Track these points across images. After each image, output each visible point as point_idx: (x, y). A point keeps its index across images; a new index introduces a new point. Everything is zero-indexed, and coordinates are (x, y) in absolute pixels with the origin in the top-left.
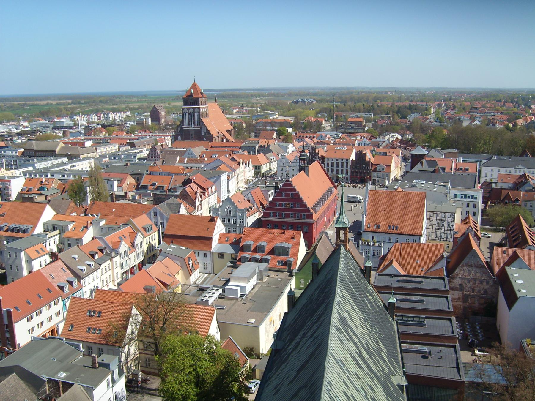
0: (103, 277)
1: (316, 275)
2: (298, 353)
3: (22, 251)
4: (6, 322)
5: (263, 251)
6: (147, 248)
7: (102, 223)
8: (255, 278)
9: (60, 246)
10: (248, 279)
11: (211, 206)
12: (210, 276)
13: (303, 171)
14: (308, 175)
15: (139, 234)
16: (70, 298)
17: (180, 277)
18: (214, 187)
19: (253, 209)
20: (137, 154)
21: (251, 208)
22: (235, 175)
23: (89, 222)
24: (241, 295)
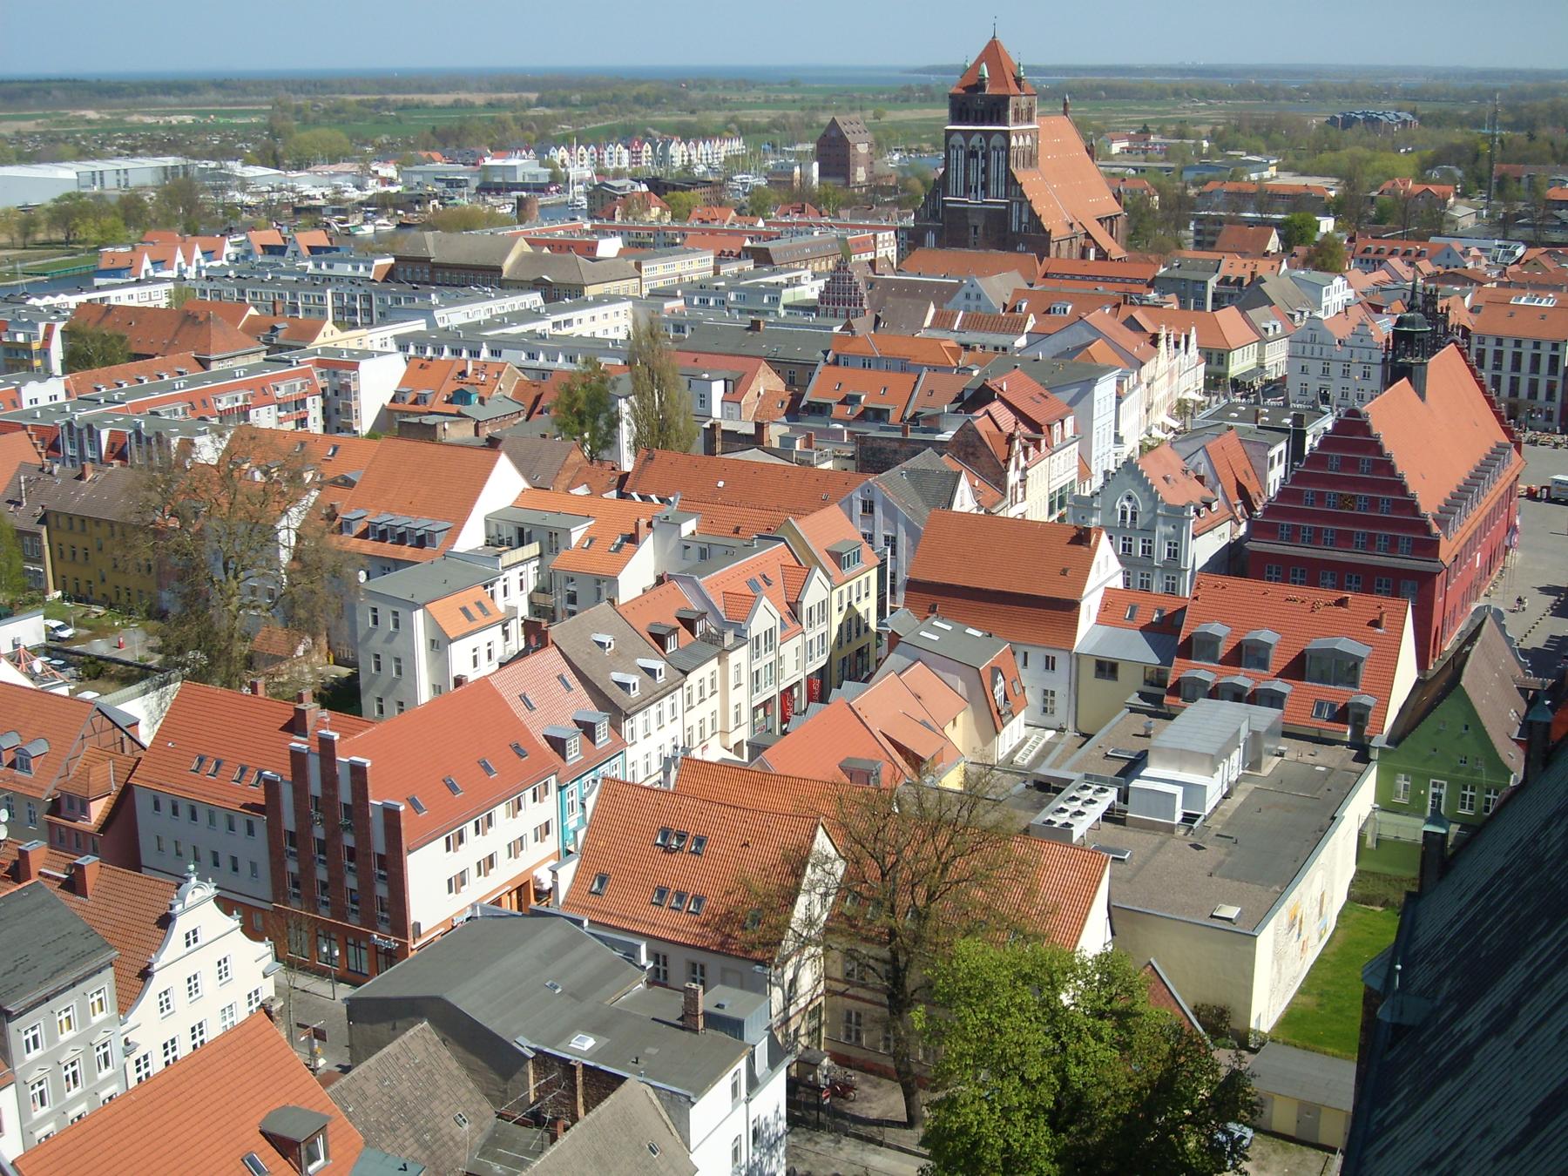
0: (693, 718)
1: (1541, 768)
2: (1518, 1046)
3: (416, 606)
4: (379, 845)
5: (1263, 664)
6: (841, 627)
7: (688, 527)
8: (1237, 756)
9: (541, 599)
10: (1213, 761)
11: (1057, 488)
12: (1064, 739)
13: (1405, 379)
14: (1422, 396)
15: (819, 572)
16: (599, 781)
17: (960, 732)
18: (1069, 422)
19: (1215, 506)
20: (784, 292)
21: (1208, 506)
22: (1139, 381)
23: (643, 522)
24: (1185, 814)
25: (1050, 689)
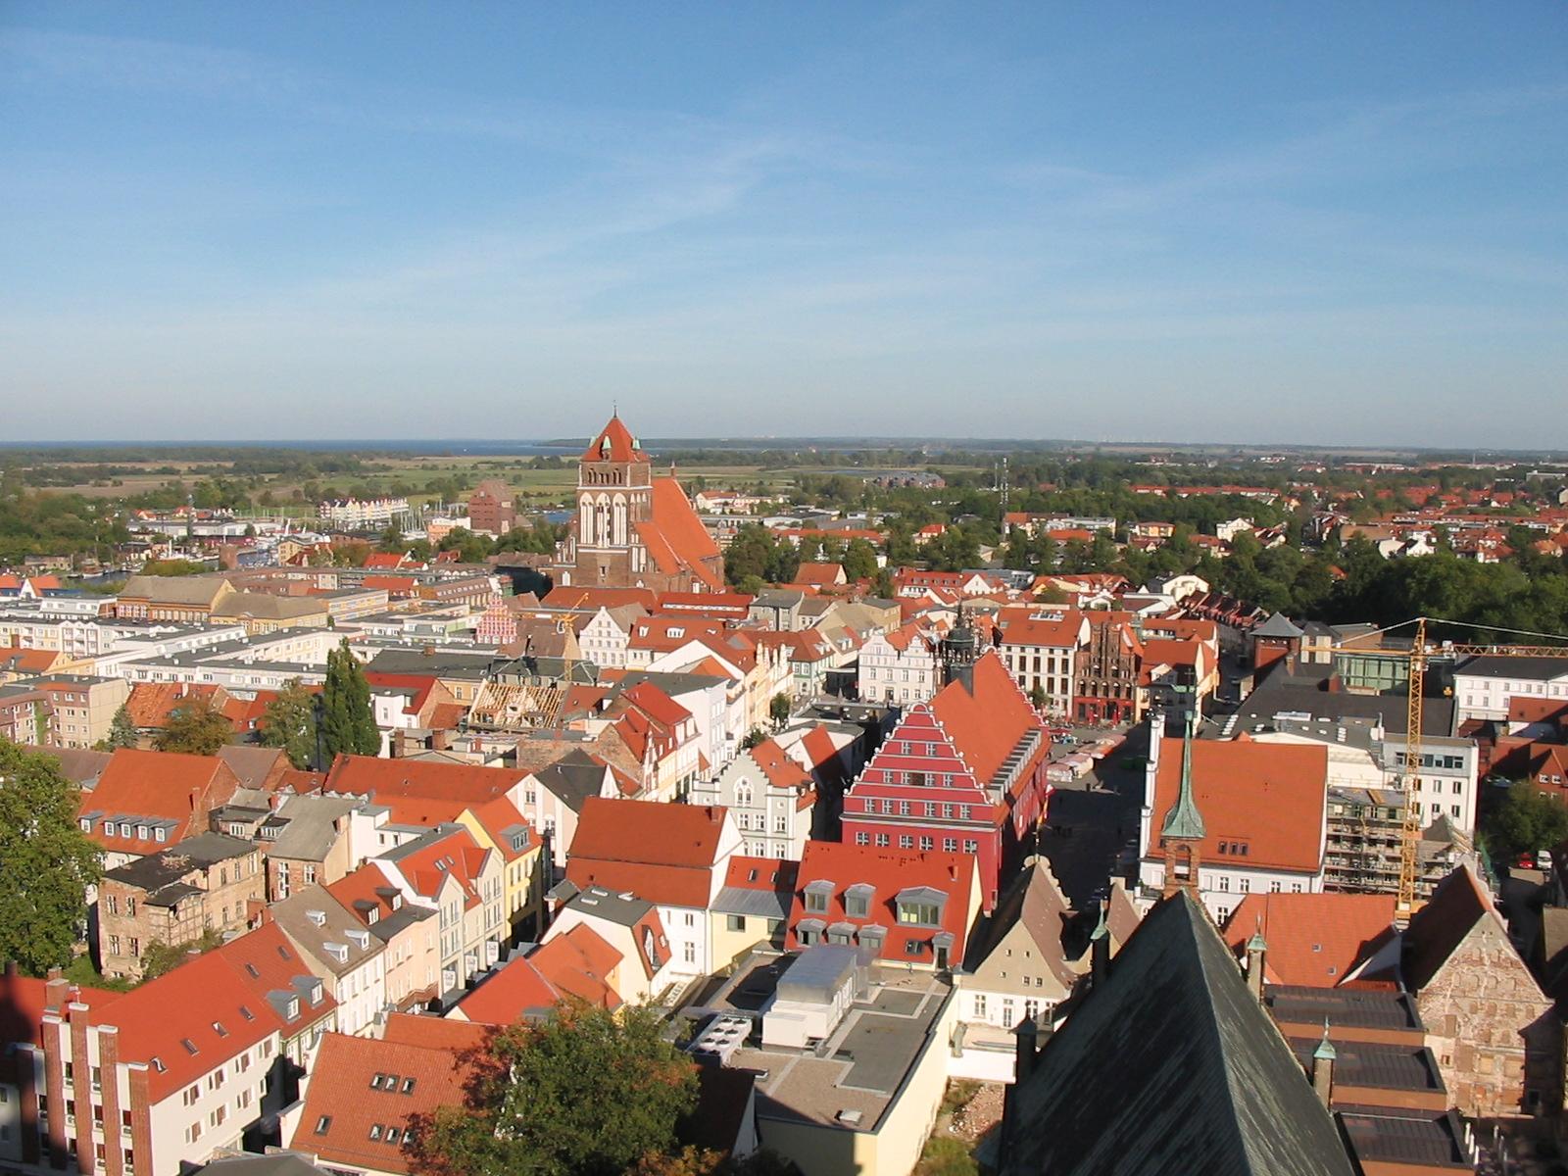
25: (690, 941)
